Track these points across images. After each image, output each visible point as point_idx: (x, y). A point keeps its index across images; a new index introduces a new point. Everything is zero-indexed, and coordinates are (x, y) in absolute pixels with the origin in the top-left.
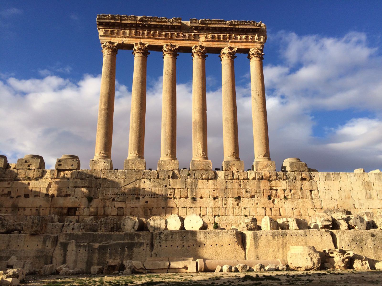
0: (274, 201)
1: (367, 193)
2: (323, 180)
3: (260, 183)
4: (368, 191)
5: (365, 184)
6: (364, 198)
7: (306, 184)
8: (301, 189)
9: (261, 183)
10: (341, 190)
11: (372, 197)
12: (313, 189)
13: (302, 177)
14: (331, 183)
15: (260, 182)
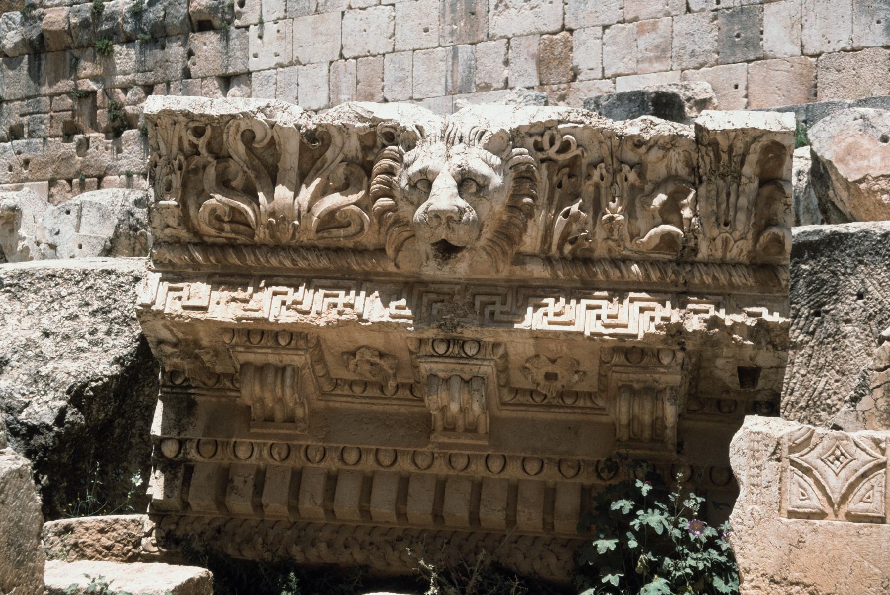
0: (84, 145)
1: (455, 57)
2: (274, 17)
3: (39, 69)
4: (465, 50)
5: (453, 11)
6: (440, 89)
7: (207, 44)
8: (187, 74)
9: (42, 68)
10: (341, 56)
11: (480, 78)
12: (231, 70)
13: (189, 16)
14: (303, 27)
15: (40, 65)
